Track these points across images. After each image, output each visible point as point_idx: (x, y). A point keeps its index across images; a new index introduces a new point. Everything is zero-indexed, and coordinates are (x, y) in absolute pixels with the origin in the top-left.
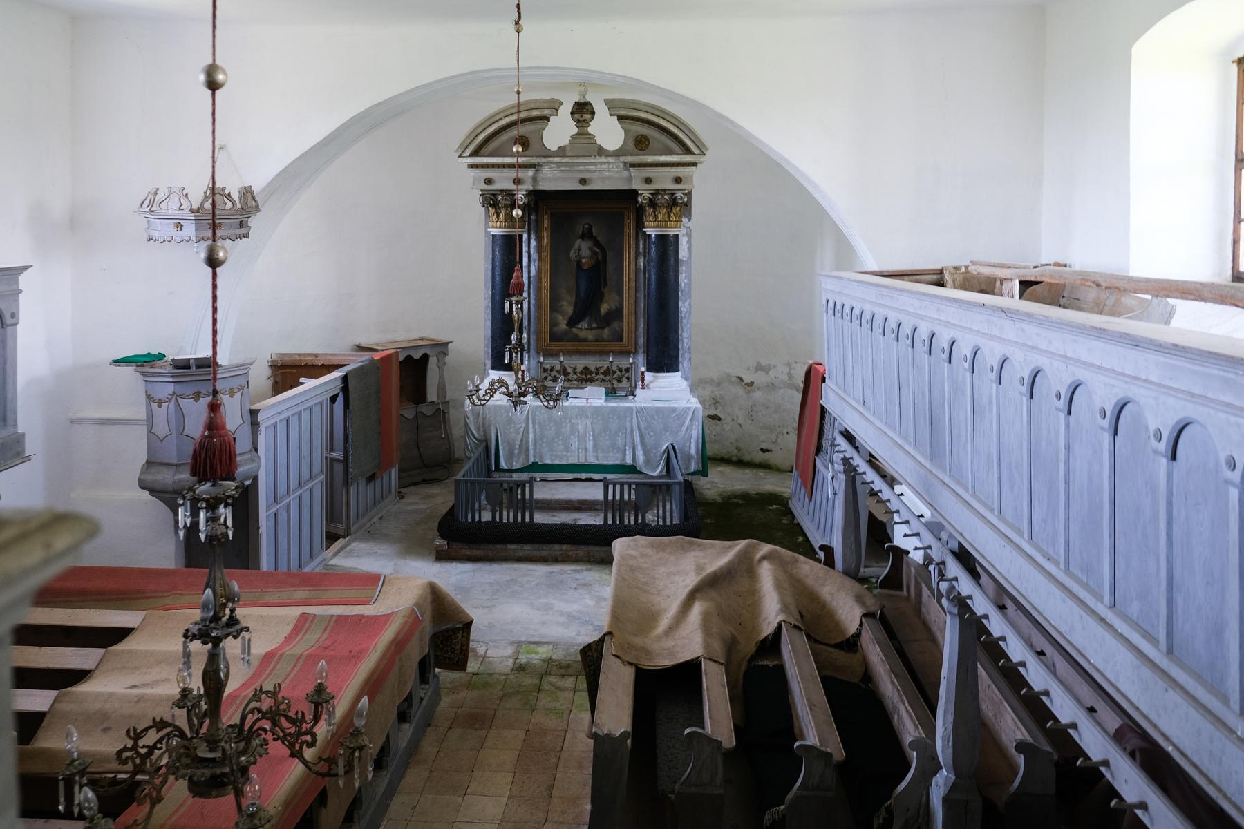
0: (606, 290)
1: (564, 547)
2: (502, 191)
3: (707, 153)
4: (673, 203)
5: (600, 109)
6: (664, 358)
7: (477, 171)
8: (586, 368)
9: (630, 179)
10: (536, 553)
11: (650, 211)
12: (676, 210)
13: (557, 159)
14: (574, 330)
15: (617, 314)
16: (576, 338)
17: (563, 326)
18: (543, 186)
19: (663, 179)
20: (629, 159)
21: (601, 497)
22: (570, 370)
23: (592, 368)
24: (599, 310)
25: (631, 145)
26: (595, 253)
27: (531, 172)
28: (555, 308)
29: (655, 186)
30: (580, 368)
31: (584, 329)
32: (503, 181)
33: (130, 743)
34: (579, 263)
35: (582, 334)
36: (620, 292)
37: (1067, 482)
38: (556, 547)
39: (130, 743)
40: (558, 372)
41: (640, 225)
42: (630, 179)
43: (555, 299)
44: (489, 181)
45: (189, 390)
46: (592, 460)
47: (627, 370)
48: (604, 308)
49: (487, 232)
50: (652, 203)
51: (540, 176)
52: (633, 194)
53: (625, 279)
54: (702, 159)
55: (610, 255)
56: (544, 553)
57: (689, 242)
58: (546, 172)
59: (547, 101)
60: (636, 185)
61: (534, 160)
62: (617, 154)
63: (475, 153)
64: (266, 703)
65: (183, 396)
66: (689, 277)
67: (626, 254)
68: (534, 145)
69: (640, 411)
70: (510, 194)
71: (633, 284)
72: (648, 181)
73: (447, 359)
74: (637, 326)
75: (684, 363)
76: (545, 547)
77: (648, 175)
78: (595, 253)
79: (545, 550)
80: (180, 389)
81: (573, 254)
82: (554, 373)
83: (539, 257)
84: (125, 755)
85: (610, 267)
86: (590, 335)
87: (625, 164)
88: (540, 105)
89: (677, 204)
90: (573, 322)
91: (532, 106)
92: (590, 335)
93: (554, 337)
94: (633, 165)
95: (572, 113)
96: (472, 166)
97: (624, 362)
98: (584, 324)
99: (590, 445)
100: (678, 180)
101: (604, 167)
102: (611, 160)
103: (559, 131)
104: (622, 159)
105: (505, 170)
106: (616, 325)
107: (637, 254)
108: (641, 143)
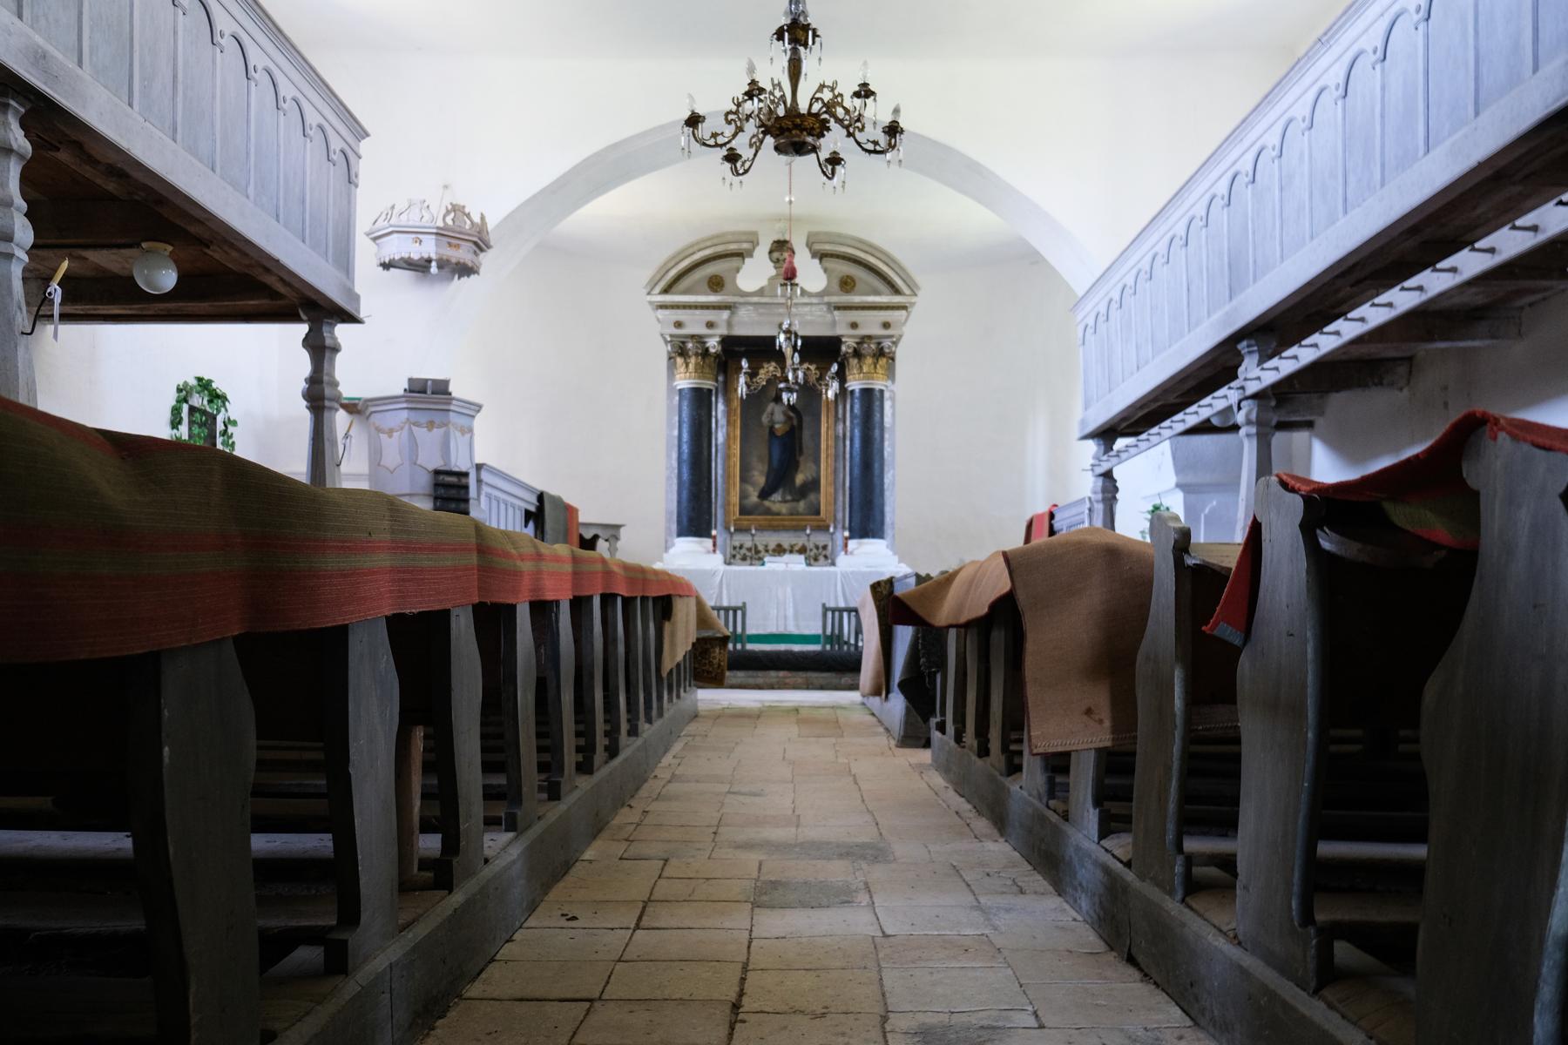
0: (802, 459)
1: (781, 674)
2: (693, 337)
3: (920, 293)
4: (880, 353)
5: (799, 244)
6: (867, 522)
7: (667, 312)
8: (779, 546)
9: (834, 324)
10: (751, 681)
11: (854, 362)
12: (883, 361)
13: (755, 299)
14: (767, 503)
15: (813, 485)
16: (768, 512)
17: (754, 498)
18: (740, 331)
19: (871, 324)
20: (835, 299)
21: (820, 632)
22: (761, 548)
23: (786, 546)
24: (793, 481)
25: (836, 287)
26: (790, 418)
27: (725, 314)
28: (744, 479)
29: (861, 332)
30: (772, 546)
31: (776, 502)
32: (695, 324)
33: (734, 108)
34: (772, 428)
35: (776, 507)
36: (817, 461)
37: (1382, 116)
38: (773, 673)
39: (734, 108)
40: (749, 550)
41: (841, 376)
42: (834, 324)
43: (745, 469)
44: (679, 325)
45: (423, 418)
46: (792, 629)
47: (825, 547)
48: (800, 479)
49: (670, 388)
50: (857, 354)
51: (736, 319)
52: (836, 342)
53: (823, 446)
54: (914, 299)
55: (806, 419)
56: (760, 681)
57: (893, 407)
58: (743, 313)
59: (745, 233)
60: (841, 330)
61: (729, 299)
62: (820, 295)
63: (666, 291)
64: (827, 96)
65: (417, 424)
66: (893, 446)
67: (823, 419)
68: (728, 286)
69: (845, 575)
70: (699, 339)
71: (832, 451)
72: (854, 325)
73: (619, 544)
74: (834, 494)
75: (888, 531)
76: (760, 674)
77: (854, 319)
78: (790, 418)
79: (760, 677)
80: (414, 416)
81: (765, 419)
82: (743, 551)
83: (728, 422)
84: (731, 117)
85: (806, 434)
86: (784, 508)
87: (829, 304)
88: (738, 237)
89: (883, 354)
90: (765, 494)
91: (730, 238)
92: (784, 508)
93: (744, 511)
94: (838, 308)
95: (771, 252)
96: (663, 306)
97: (820, 539)
98: (777, 497)
99: (790, 612)
100: (886, 325)
101: (807, 309)
102: (814, 300)
103: (755, 274)
104: (826, 299)
105: (698, 312)
106: (812, 497)
107: (836, 419)
108: (847, 284)
